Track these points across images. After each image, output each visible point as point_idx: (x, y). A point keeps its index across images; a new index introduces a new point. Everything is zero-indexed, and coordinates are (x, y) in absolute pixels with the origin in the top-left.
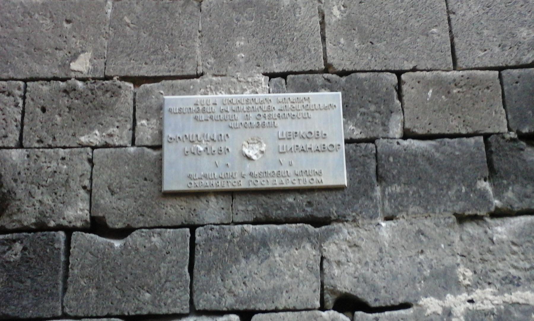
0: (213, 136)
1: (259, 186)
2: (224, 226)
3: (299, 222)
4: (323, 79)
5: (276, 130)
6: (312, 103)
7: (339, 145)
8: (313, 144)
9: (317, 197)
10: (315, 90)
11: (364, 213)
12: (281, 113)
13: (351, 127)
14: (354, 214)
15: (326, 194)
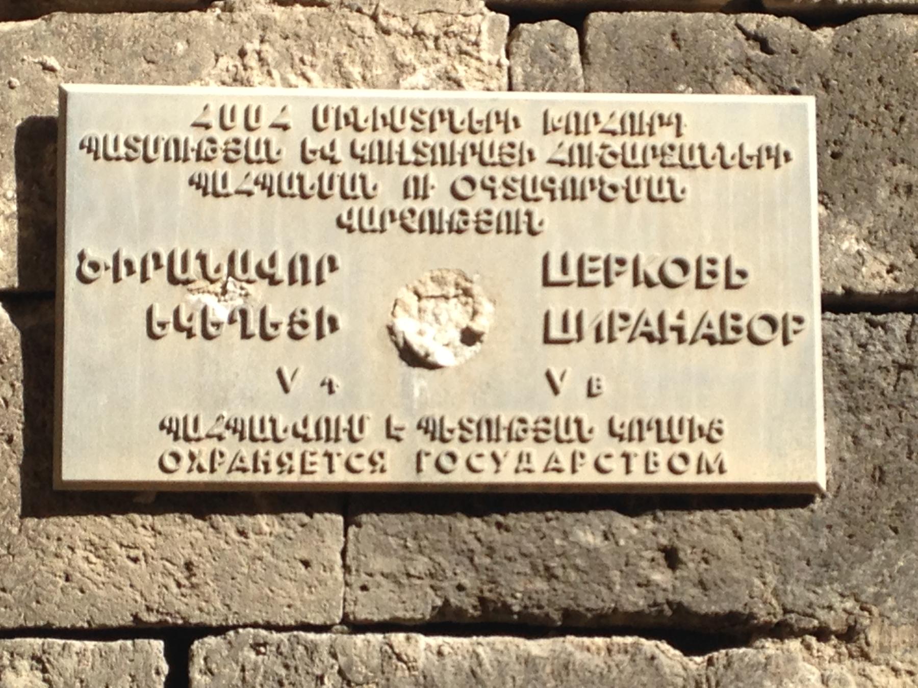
0: (272, 261)
1: (459, 476)
2: (311, 636)
3: (622, 632)
4: (740, 35)
5: (539, 246)
6: (690, 138)
7: (799, 320)
8: (691, 305)
9: (695, 528)
10: (705, 82)
11: (890, 602)
12: (559, 174)
13: (850, 244)
14: (849, 604)
15: (739, 518)
